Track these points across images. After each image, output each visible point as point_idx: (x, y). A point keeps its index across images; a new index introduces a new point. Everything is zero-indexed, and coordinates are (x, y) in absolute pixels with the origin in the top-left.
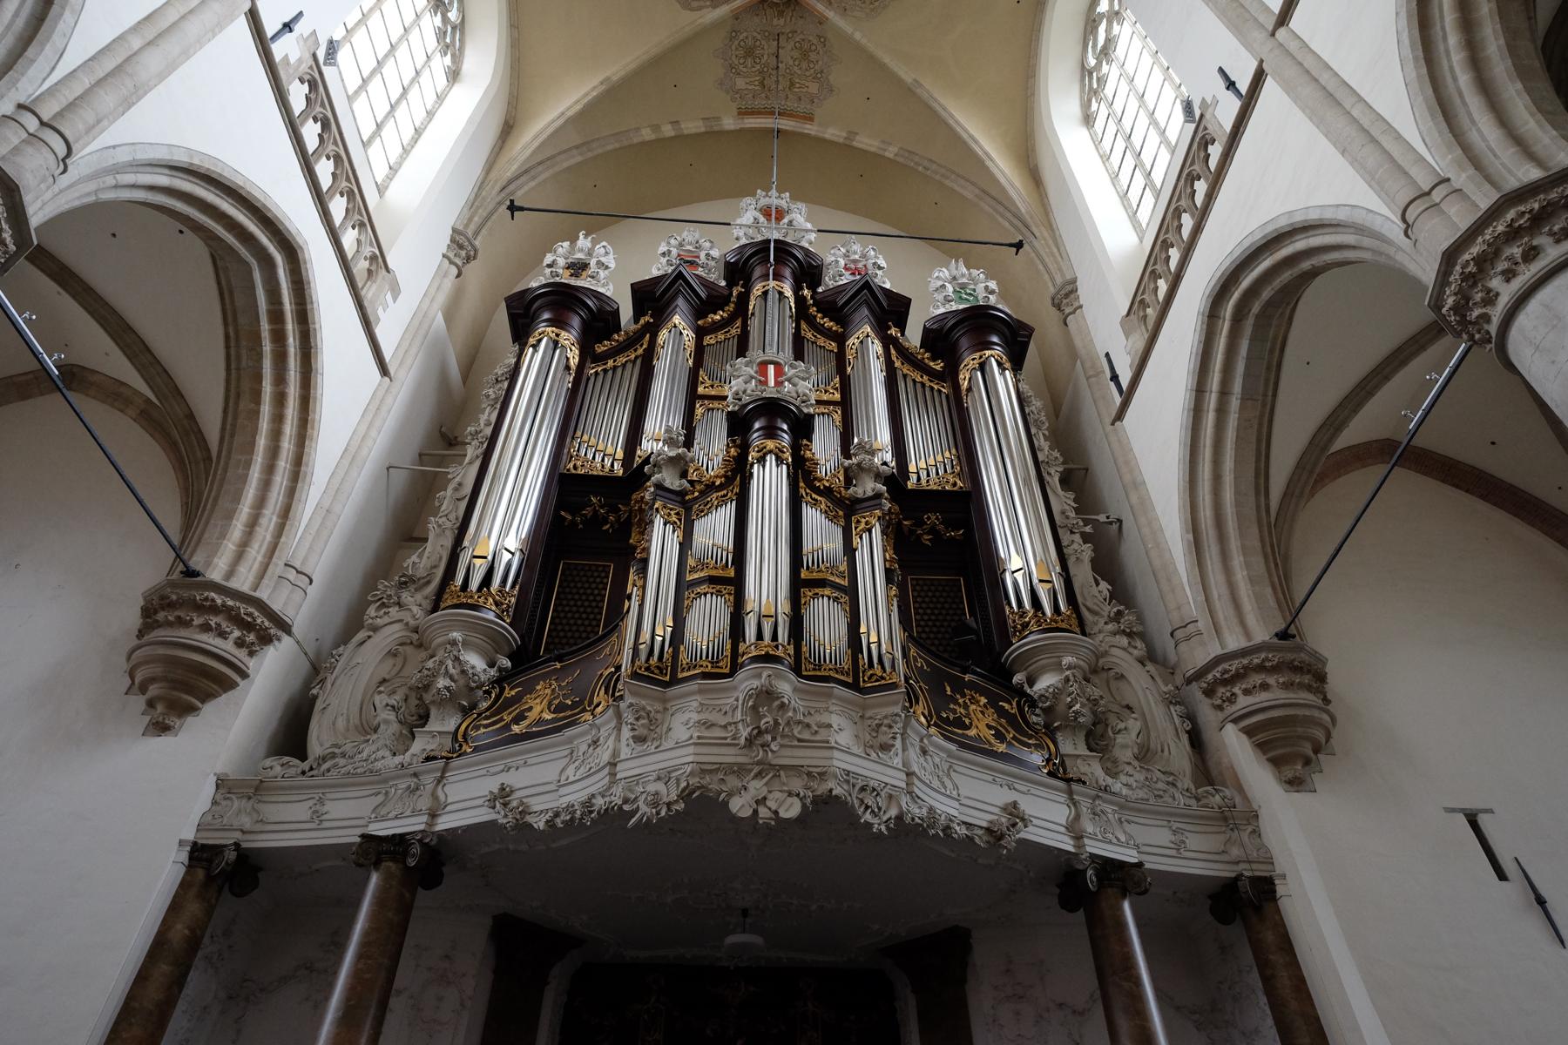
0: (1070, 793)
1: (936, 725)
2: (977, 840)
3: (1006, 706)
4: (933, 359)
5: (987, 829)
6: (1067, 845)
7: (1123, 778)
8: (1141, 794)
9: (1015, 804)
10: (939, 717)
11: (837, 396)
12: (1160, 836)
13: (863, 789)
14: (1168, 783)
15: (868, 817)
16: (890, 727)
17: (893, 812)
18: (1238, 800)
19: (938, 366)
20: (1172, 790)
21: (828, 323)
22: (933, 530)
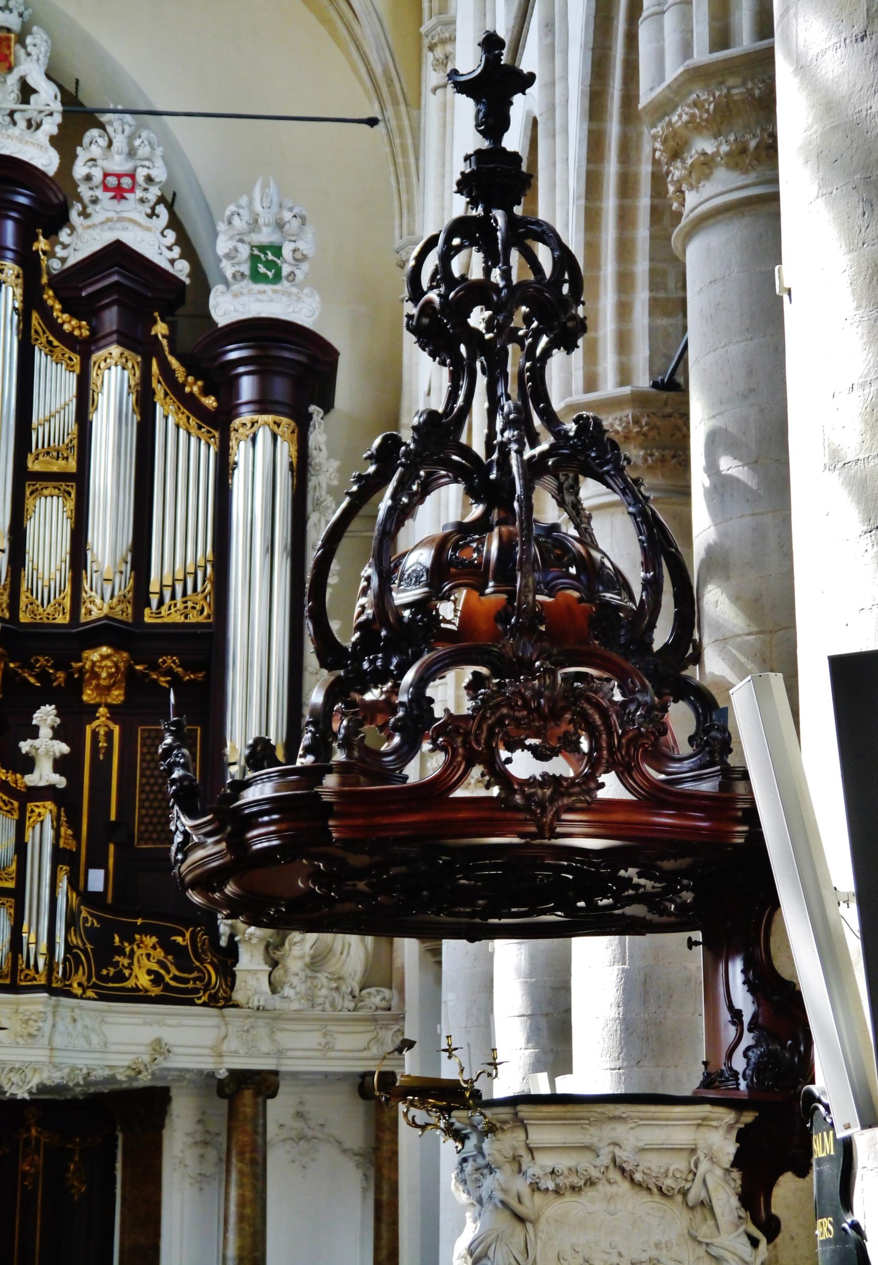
0: (223, 1017)
1: (95, 986)
2: (119, 1077)
3: (179, 939)
4: (206, 392)
5: (129, 1067)
6: (207, 1064)
7: (287, 991)
8: (295, 1006)
9: (158, 1041)
10: (100, 977)
11: (72, 466)
12: (312, 1039)
13: (11, 1070)
14: (331, 989)
15: (14, 1090)
16: (36, 1021)
17: (34, 1082)
18: (394, 1003)
19: (210, 402)
20: (335, 994)
21: (69, 323)
22: (169, 672)
